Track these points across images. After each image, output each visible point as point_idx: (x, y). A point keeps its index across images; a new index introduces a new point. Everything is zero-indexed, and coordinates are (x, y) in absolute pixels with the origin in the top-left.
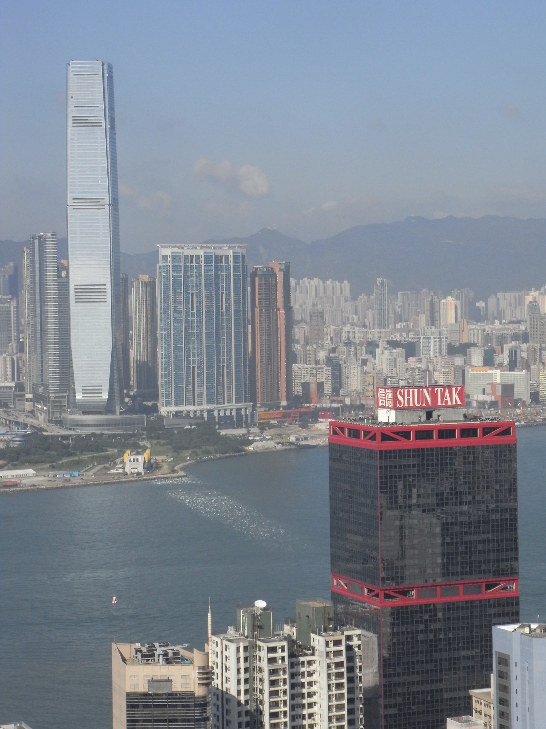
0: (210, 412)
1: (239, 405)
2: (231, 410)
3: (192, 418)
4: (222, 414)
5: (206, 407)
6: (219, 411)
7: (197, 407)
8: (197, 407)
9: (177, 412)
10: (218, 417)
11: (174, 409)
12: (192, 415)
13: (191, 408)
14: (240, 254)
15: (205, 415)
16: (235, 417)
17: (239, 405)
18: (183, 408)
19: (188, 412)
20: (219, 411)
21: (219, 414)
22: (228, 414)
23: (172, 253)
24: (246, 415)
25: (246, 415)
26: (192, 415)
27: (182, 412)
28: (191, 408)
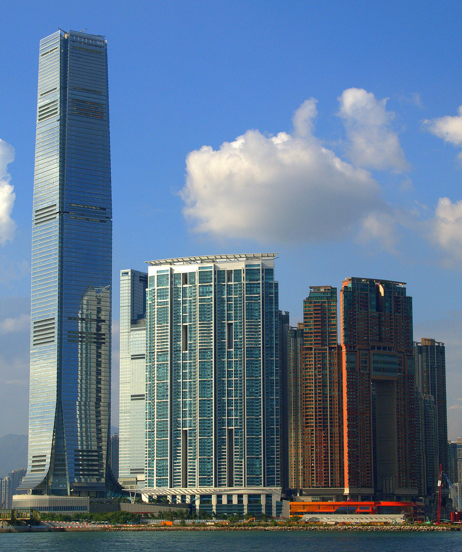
0: (205, 498)
1: (254, 490)
2: (240, 496)
3: (179, 505)
4: (225, 501)
5: (197, 490)
6: (219, 497)
7: (189, 491)
8: (189, 491)
9: (159, 497)
10: (217, 506)
11: (156, 491)
12: (179, 501)
13: (179, 490)
14: (260, 268)
15: (197, 503)
16: (245, 507)
17: (254, 490)
18: (167, 491)
19: (174, 497)
20: (219, 497)
21: (219, 501)
22: (235, 501)
23: (157, 272)
24: (269, 506)
25: (269, 506)
26: (179, 501)
27: (166, 496)
28: (179, 490)
